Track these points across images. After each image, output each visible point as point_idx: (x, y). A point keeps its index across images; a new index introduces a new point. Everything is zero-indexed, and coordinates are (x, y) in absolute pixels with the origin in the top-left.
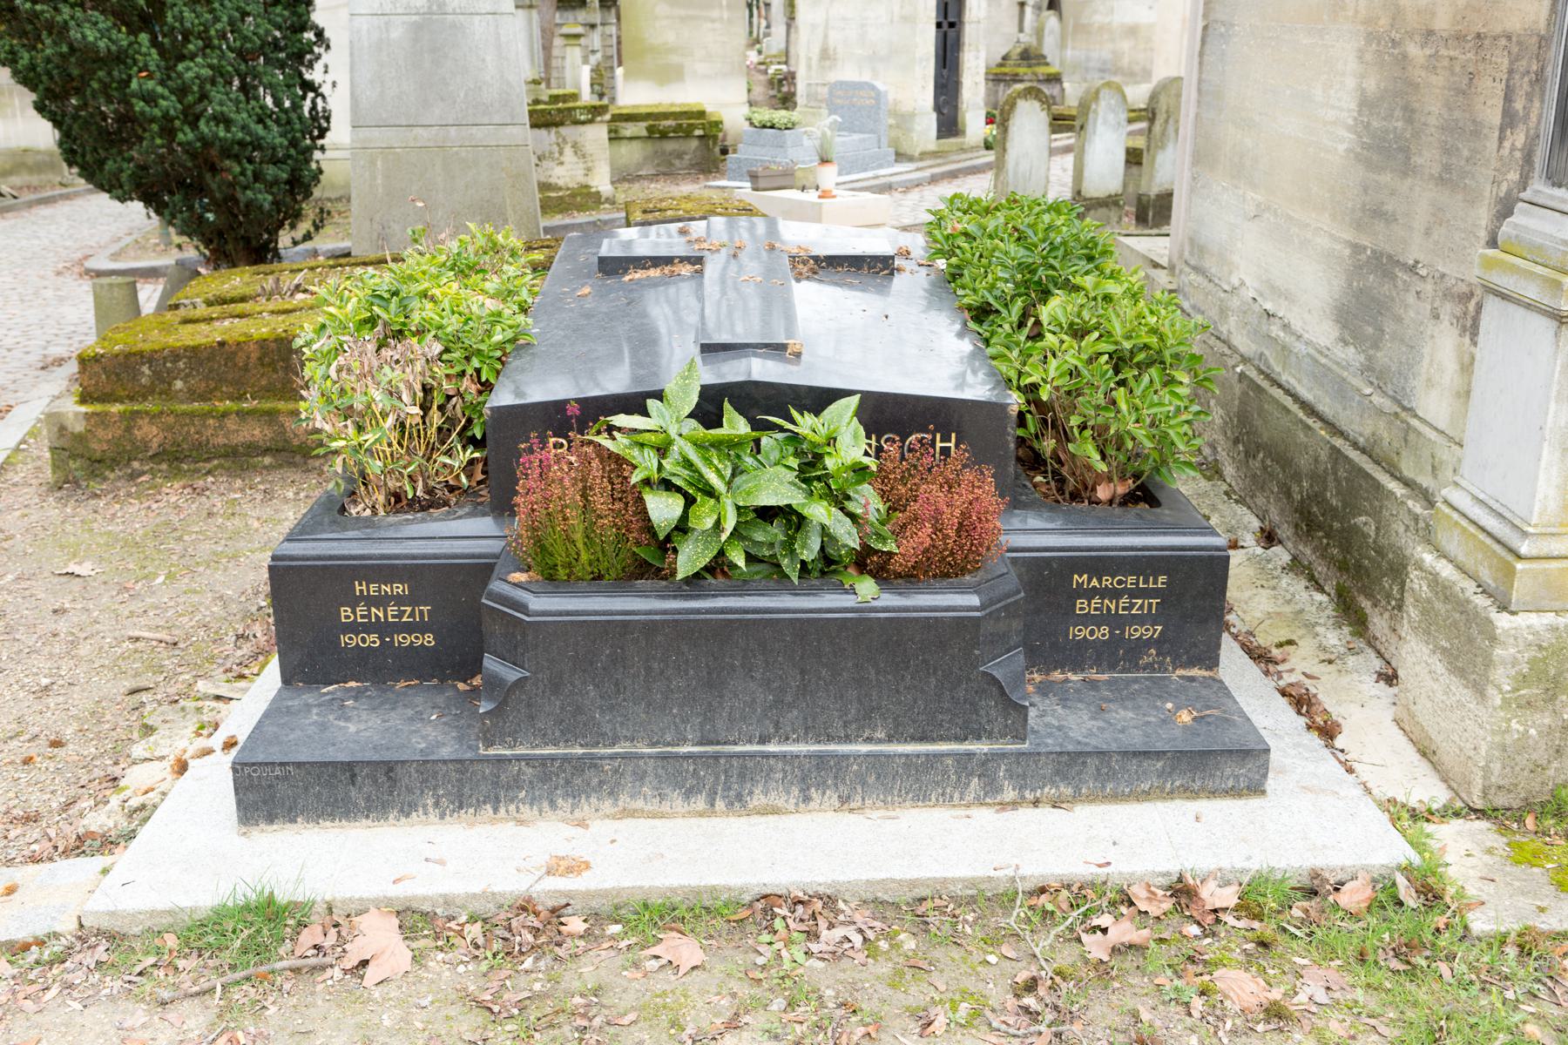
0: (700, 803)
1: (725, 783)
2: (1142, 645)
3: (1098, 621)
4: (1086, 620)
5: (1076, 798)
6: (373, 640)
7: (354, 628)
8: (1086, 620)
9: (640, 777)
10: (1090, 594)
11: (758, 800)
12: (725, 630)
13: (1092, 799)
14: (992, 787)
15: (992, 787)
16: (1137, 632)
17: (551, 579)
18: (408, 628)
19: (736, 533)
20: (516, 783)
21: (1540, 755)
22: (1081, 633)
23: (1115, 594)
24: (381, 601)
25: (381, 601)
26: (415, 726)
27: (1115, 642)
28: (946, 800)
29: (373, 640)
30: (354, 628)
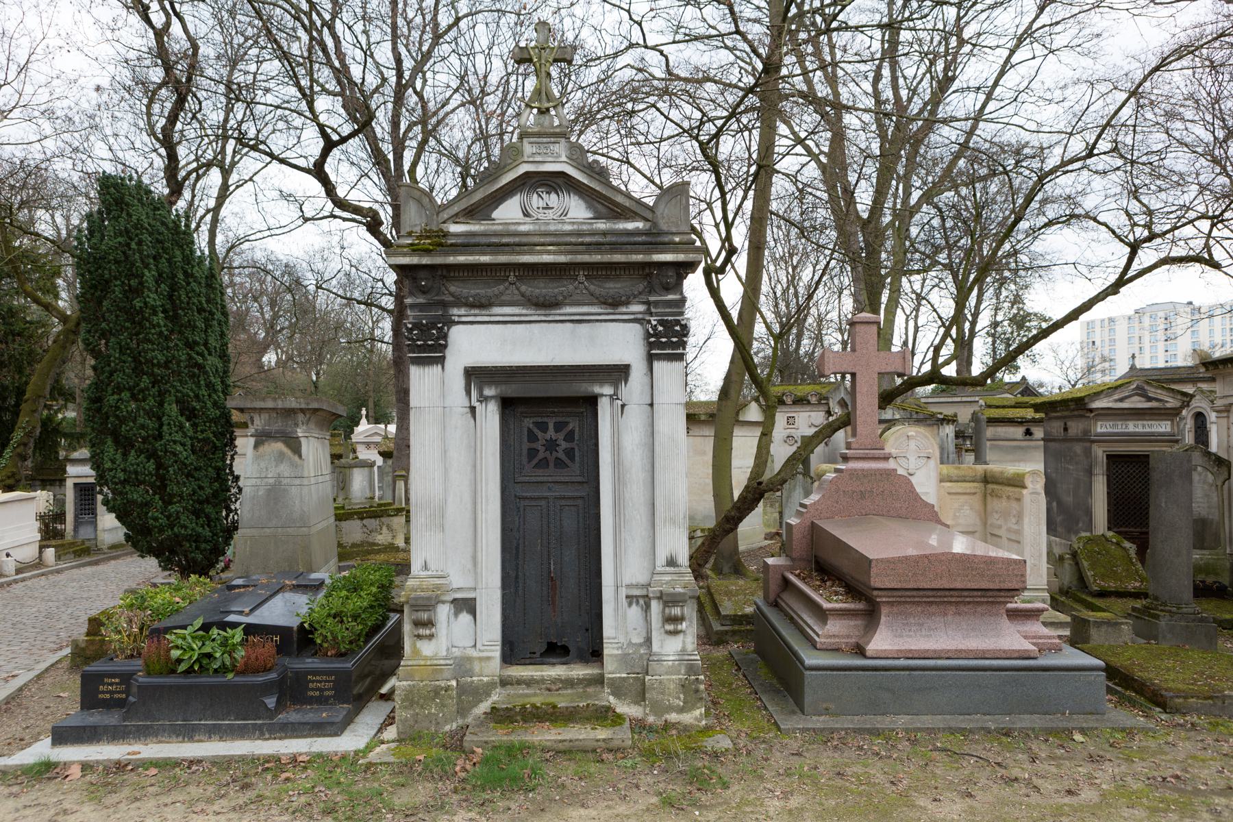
0: (180, 739)
1: (188, 733)
2: (328, 698)
3: (317, 689)
4: (313, 689)
5: (286, 737)
6: (108, 696)
7: (103, 692)
8: (313, 689)
9: (164, 731)
10: (313, 682)
11: (197, 738)
12: (190, 687)
13: (291, 737)
14: (262, 734)
15: (262, 734)
16: (327, 693)
17: (149, 674)
18: (118, 692)
19: (197, 660)
20: (130, 733)
21: (412, 723)
22: (311, 693)
23: (320, 682)
24: (111, 684)
25: (111, 684)
26: (112, 719)
27: (321, 696)
28: (249, 738)
29: (108, 696)
30: (103, 692)
